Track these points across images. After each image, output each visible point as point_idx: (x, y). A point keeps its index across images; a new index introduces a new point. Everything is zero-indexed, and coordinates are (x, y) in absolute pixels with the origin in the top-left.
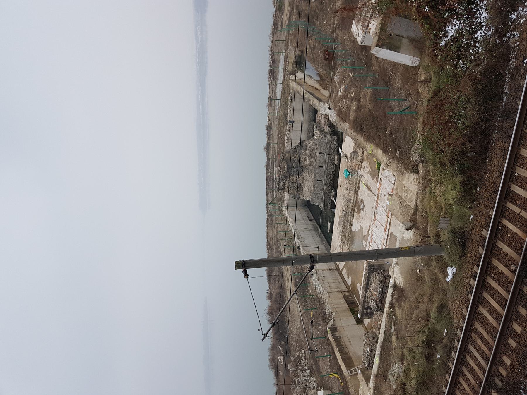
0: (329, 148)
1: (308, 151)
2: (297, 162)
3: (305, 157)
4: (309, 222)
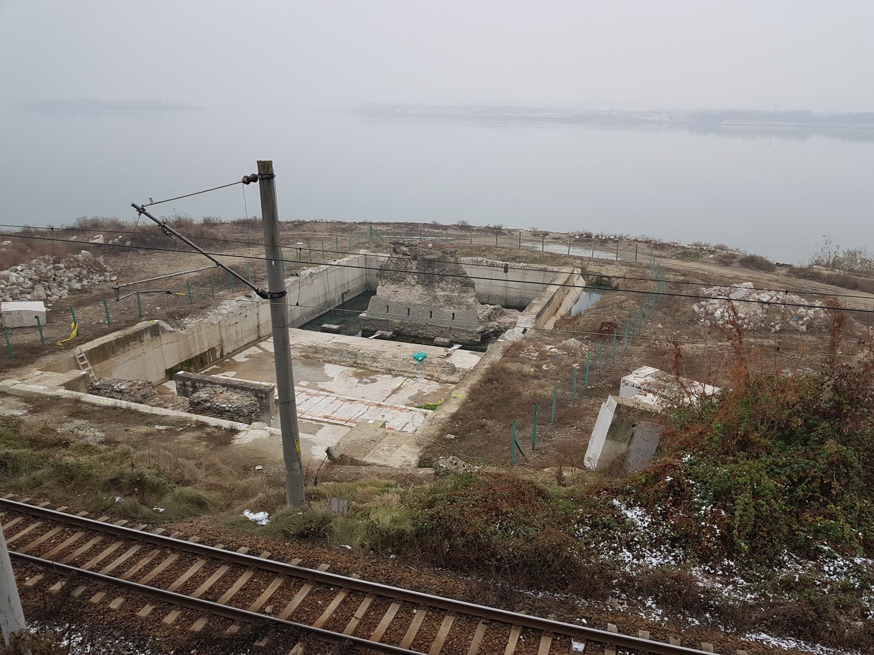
0: (461, 328)
4: (340, 294)
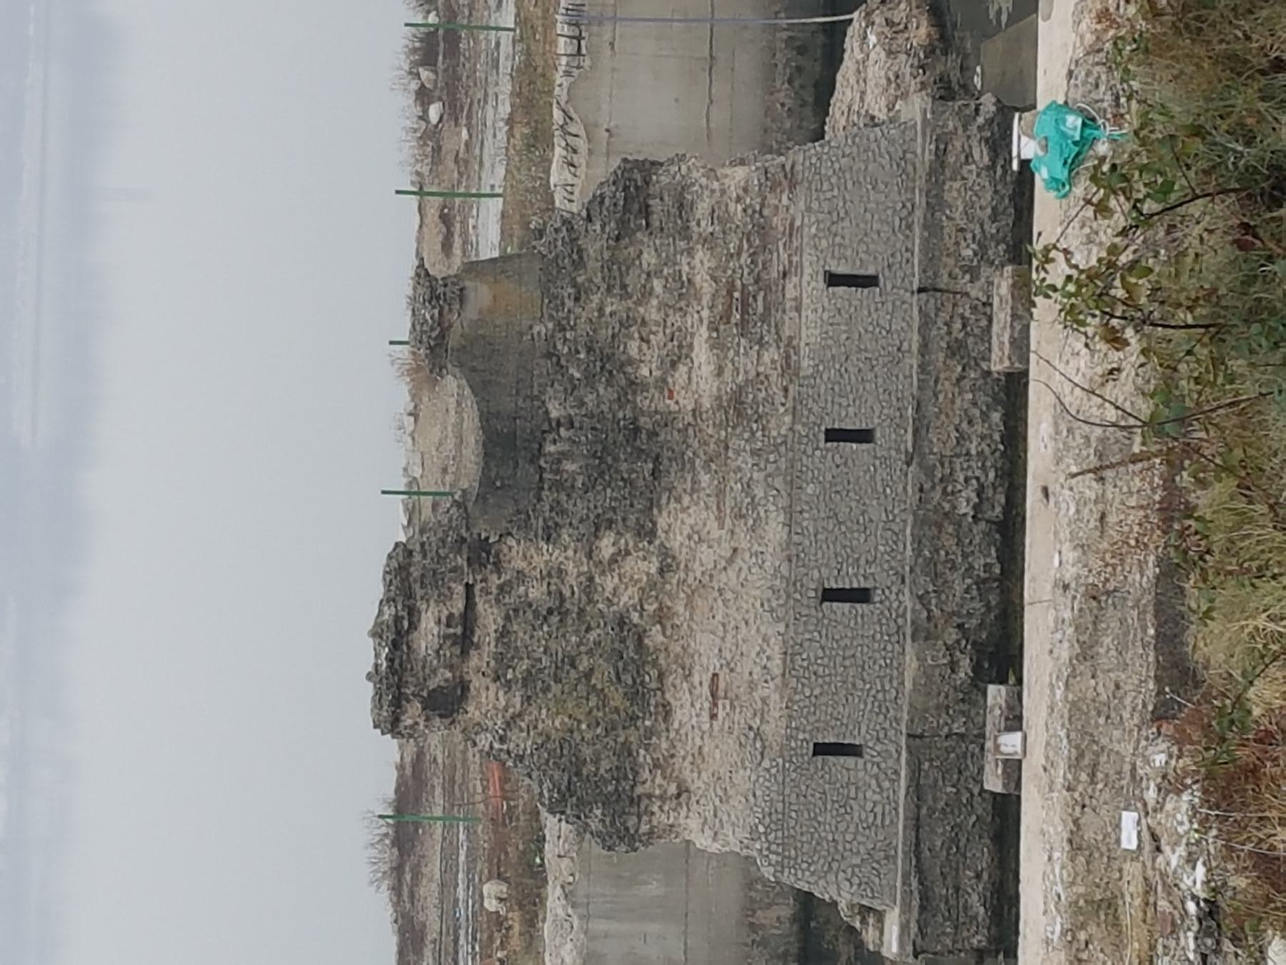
0: (919, 213)
1: (701, 254)
2: (590, 379)
3: (675, 318)
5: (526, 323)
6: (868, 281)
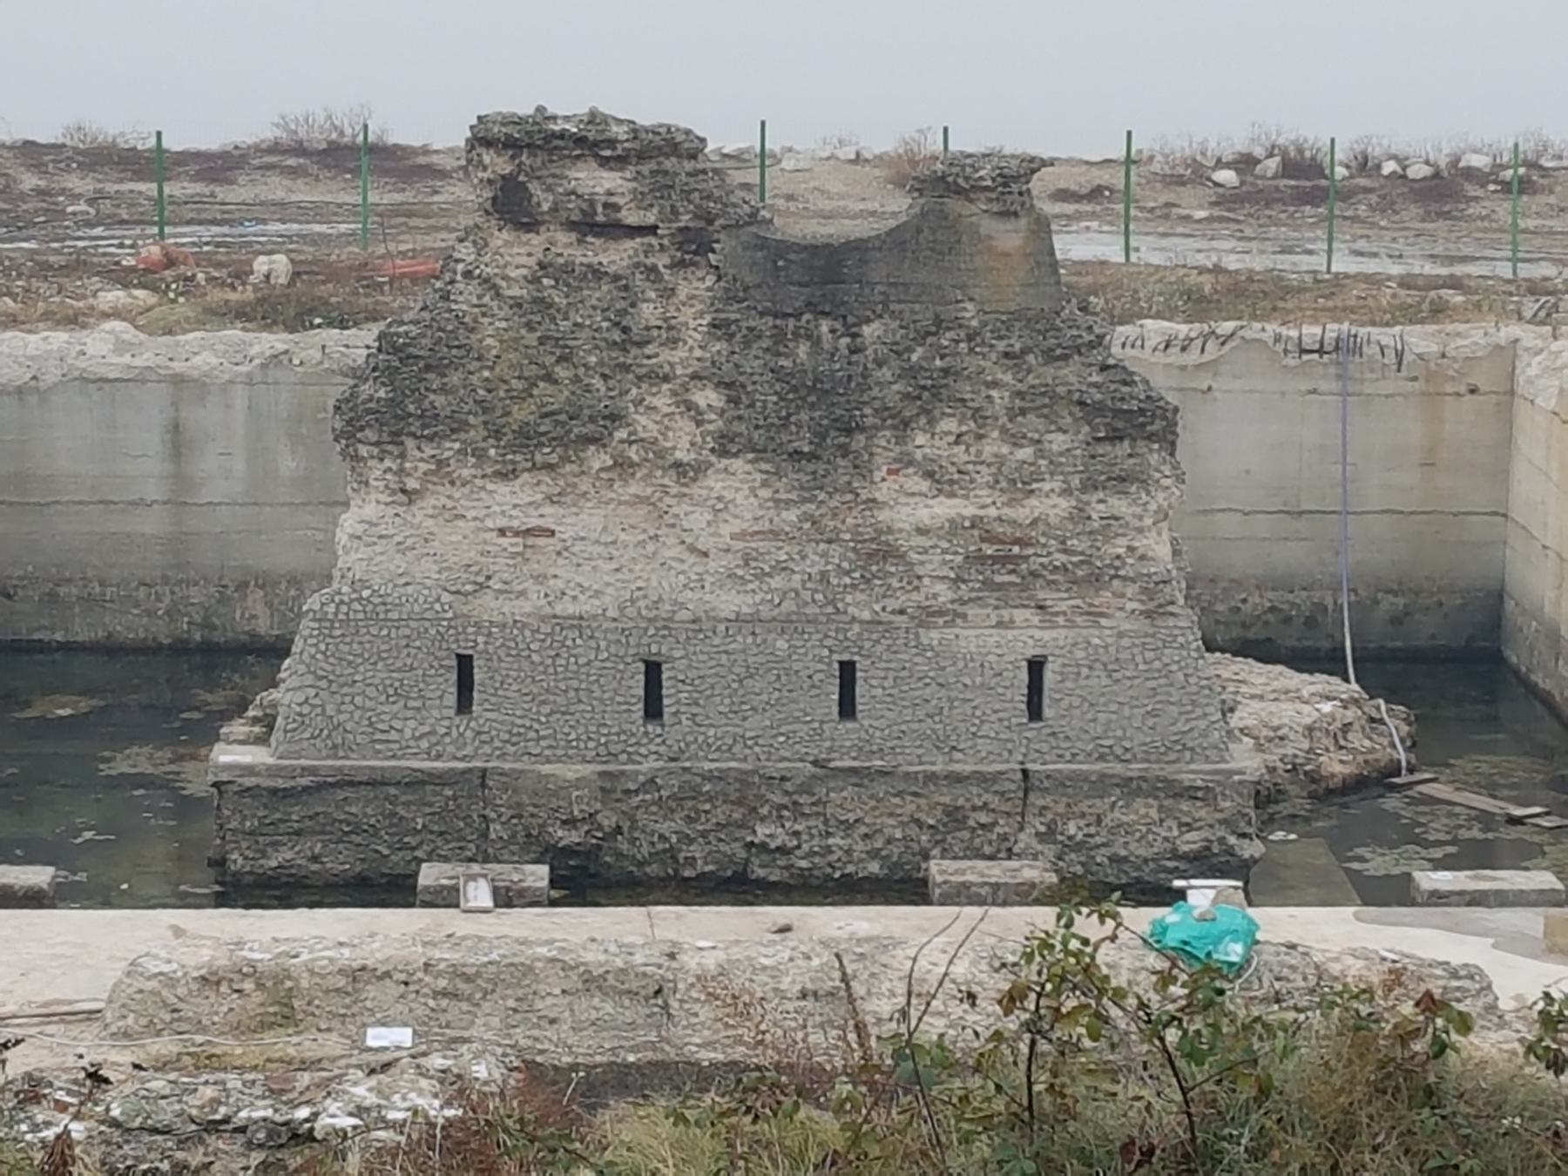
0: (1118, 768)
1: (1065, 504)
2: (910, 372)
3: (986, 474)
5: (976, 292)
6: (1035, 710)
